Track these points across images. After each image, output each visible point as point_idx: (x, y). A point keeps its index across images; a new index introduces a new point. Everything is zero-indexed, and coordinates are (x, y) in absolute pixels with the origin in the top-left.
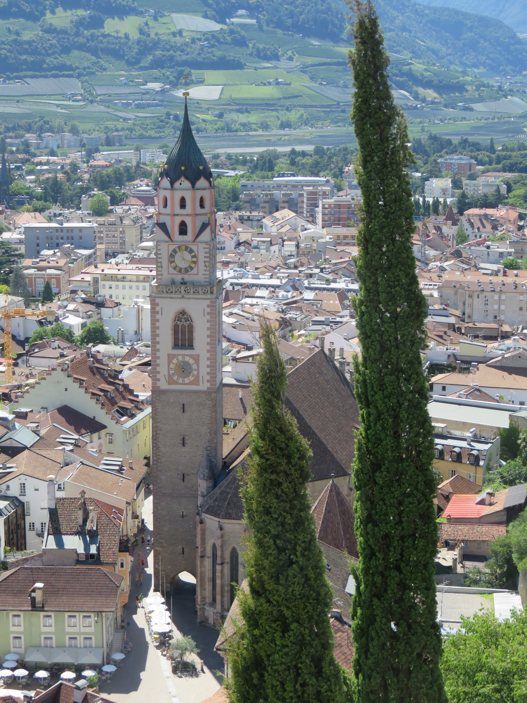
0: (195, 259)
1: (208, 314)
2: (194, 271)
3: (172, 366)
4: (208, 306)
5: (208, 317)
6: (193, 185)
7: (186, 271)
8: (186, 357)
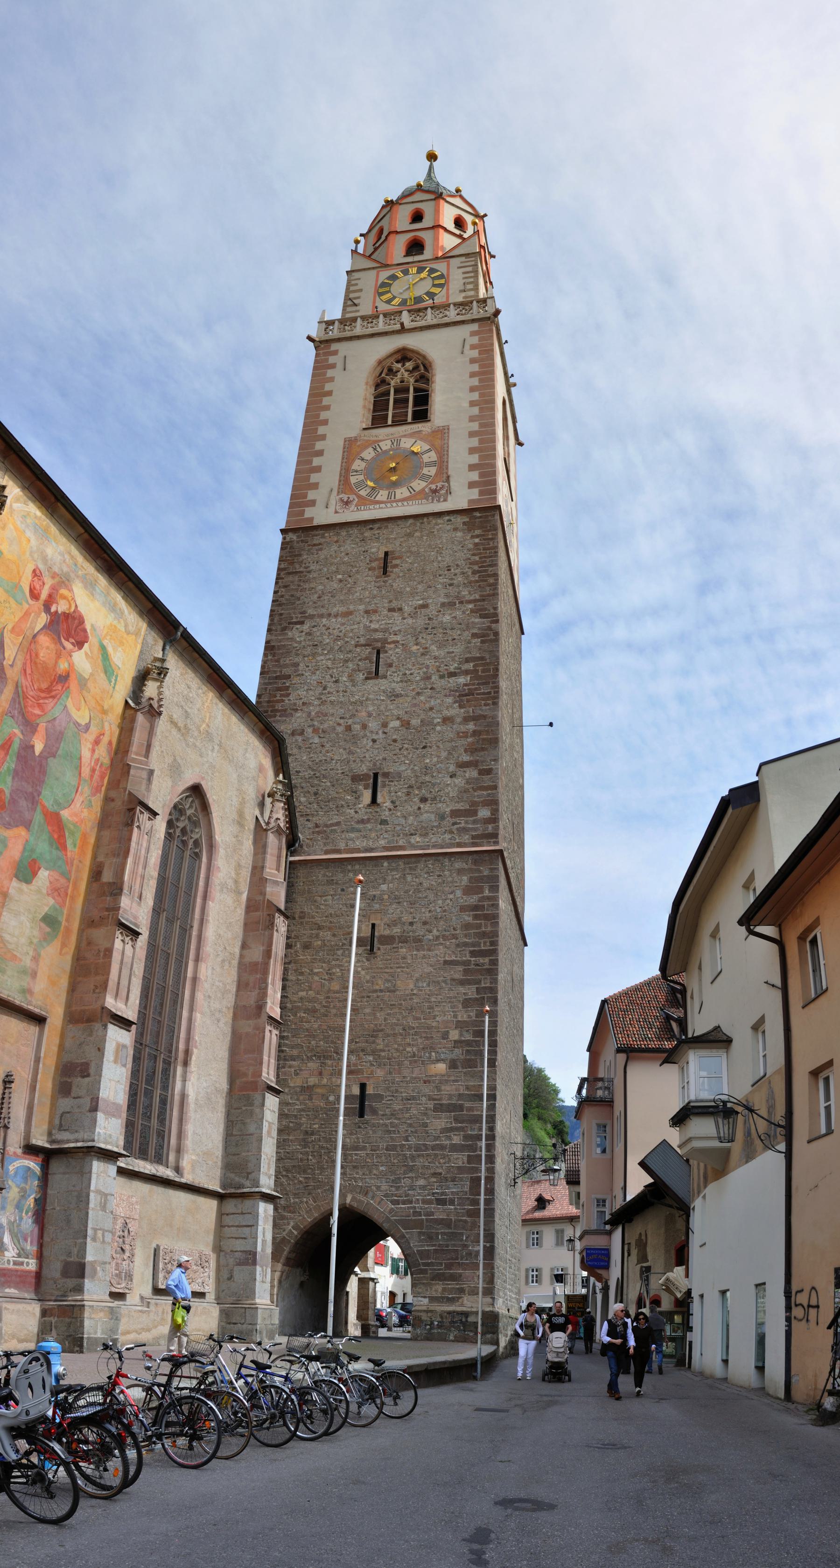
0: (442, 281)
8: (403, 440)
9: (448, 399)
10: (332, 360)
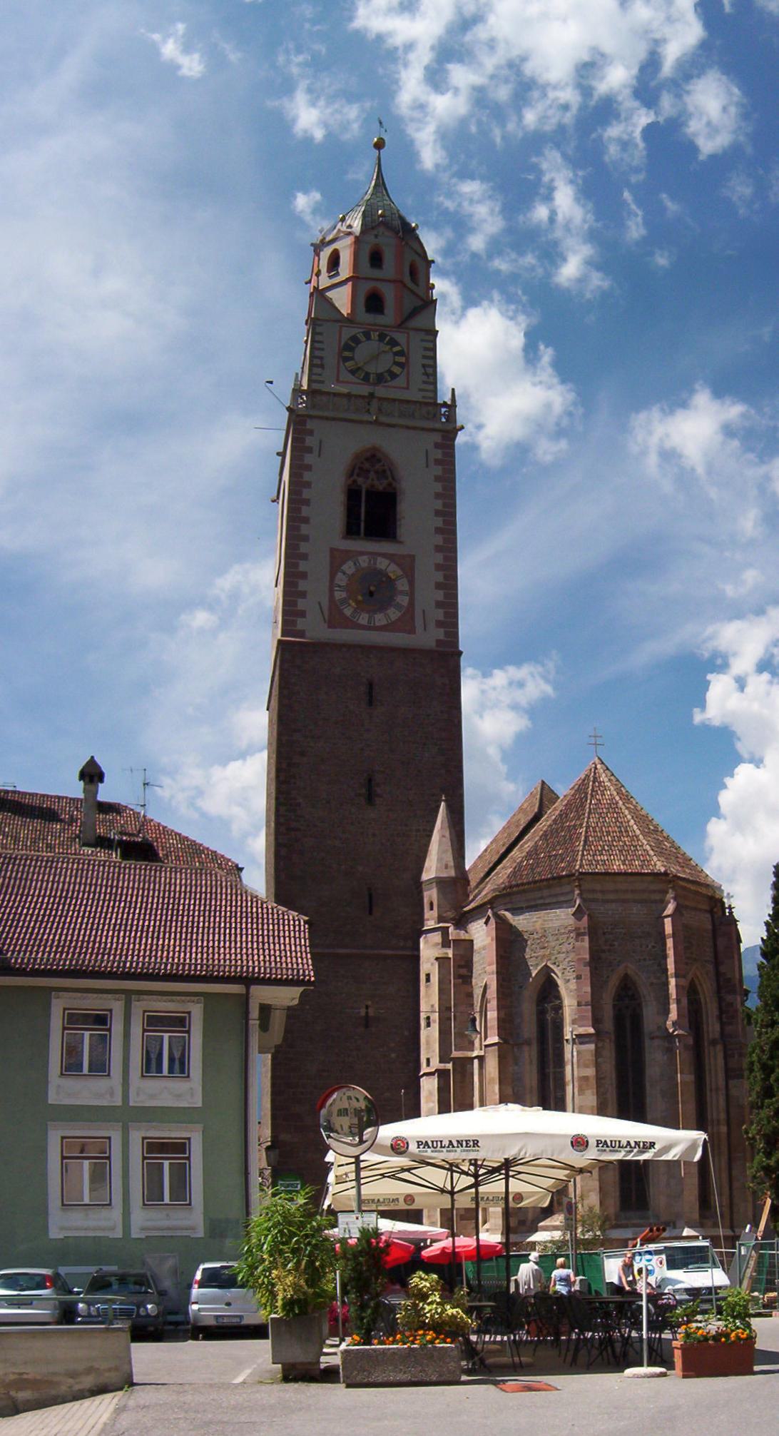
0: (403, 360)
2: (401, 381)
3: (341, 579)
7: (380, 379)
8: (379, 559)
9: (413, 514)
10: (309, 441)
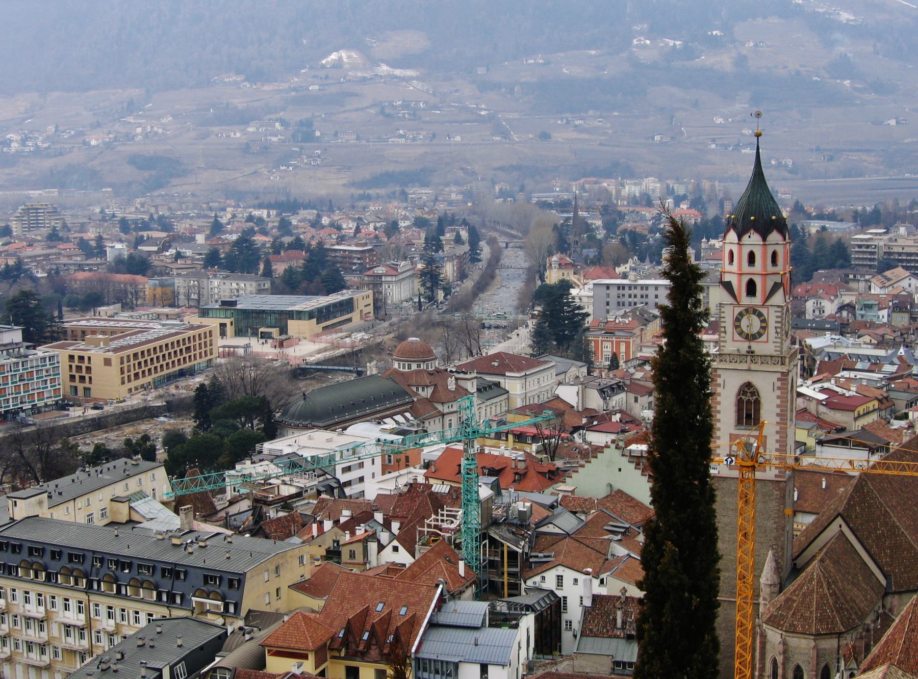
1: (779, 388)
2: (764, 338)
4: (779, 379)
5: (778, 393)
6: (764, 239)
